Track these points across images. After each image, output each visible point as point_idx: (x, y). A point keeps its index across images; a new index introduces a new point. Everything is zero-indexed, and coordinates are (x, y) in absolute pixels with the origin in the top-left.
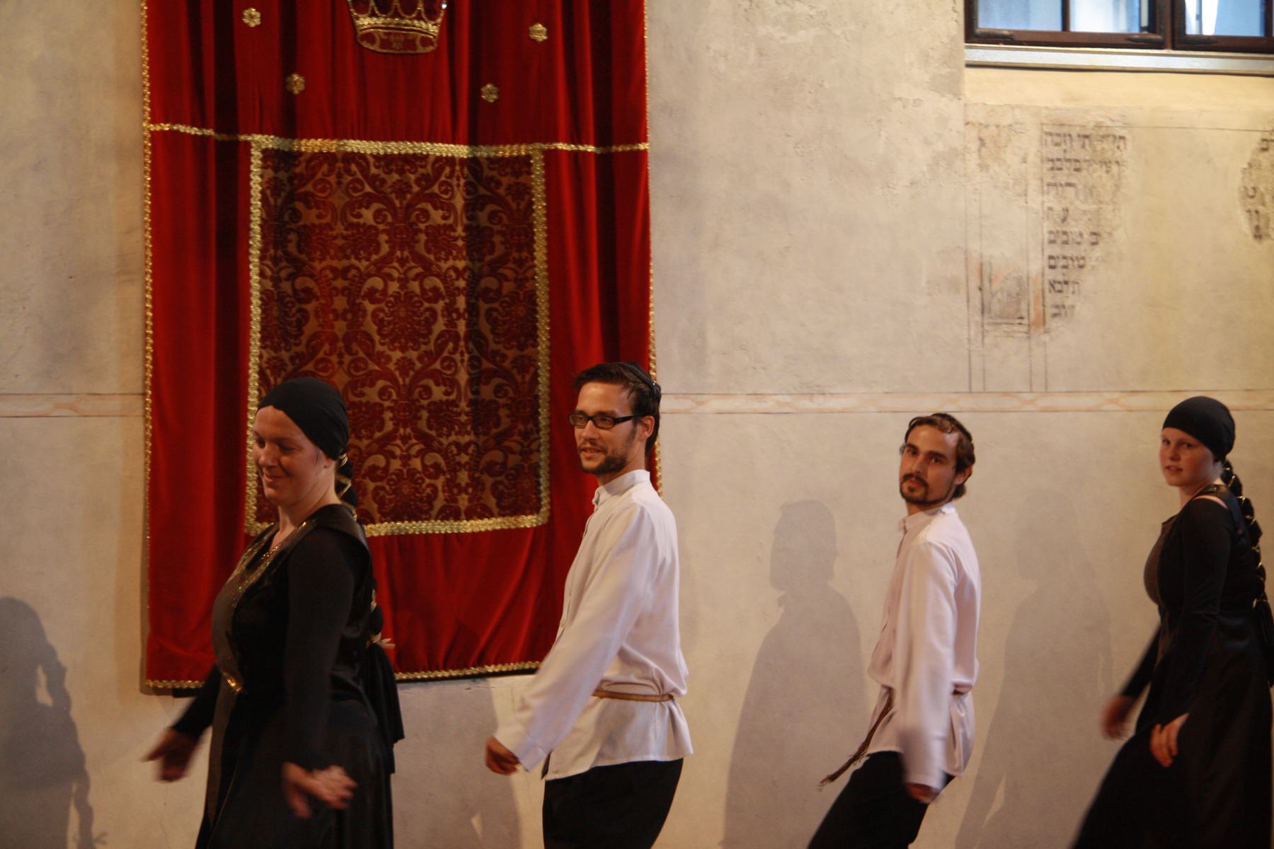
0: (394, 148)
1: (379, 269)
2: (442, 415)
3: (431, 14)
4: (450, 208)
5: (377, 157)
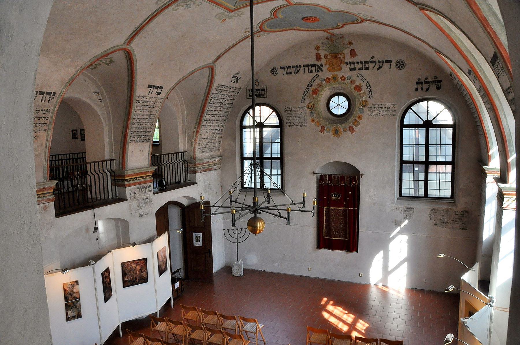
0: (336, 208)
1: (333, 218)
2: (339, 230)
3: (339, 197)
4: (340, 213)
5: (333, 209)
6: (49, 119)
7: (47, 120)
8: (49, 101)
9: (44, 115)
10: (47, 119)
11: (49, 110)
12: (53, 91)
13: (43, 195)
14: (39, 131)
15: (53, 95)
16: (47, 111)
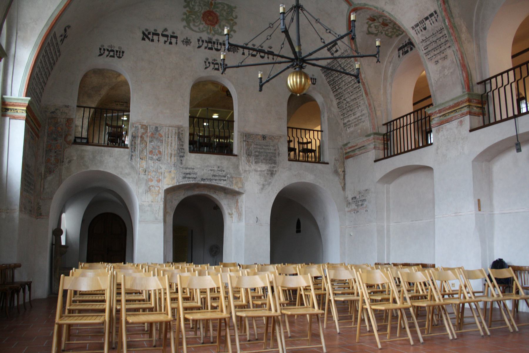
6: (447, 35)
7: (446, 37)
8: (436, 20)
9: (441, 35)
10: (445, 36)
11: (442, 28)
12: (432, 11)
13: (459, 110)
14: (445, 50)
15: (435, 14)
16: (441, 30)
